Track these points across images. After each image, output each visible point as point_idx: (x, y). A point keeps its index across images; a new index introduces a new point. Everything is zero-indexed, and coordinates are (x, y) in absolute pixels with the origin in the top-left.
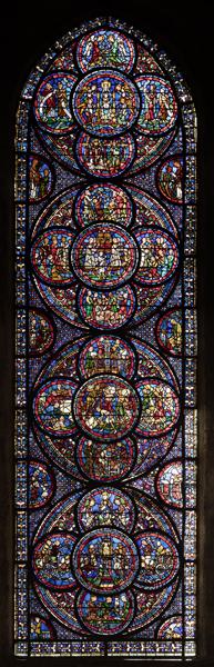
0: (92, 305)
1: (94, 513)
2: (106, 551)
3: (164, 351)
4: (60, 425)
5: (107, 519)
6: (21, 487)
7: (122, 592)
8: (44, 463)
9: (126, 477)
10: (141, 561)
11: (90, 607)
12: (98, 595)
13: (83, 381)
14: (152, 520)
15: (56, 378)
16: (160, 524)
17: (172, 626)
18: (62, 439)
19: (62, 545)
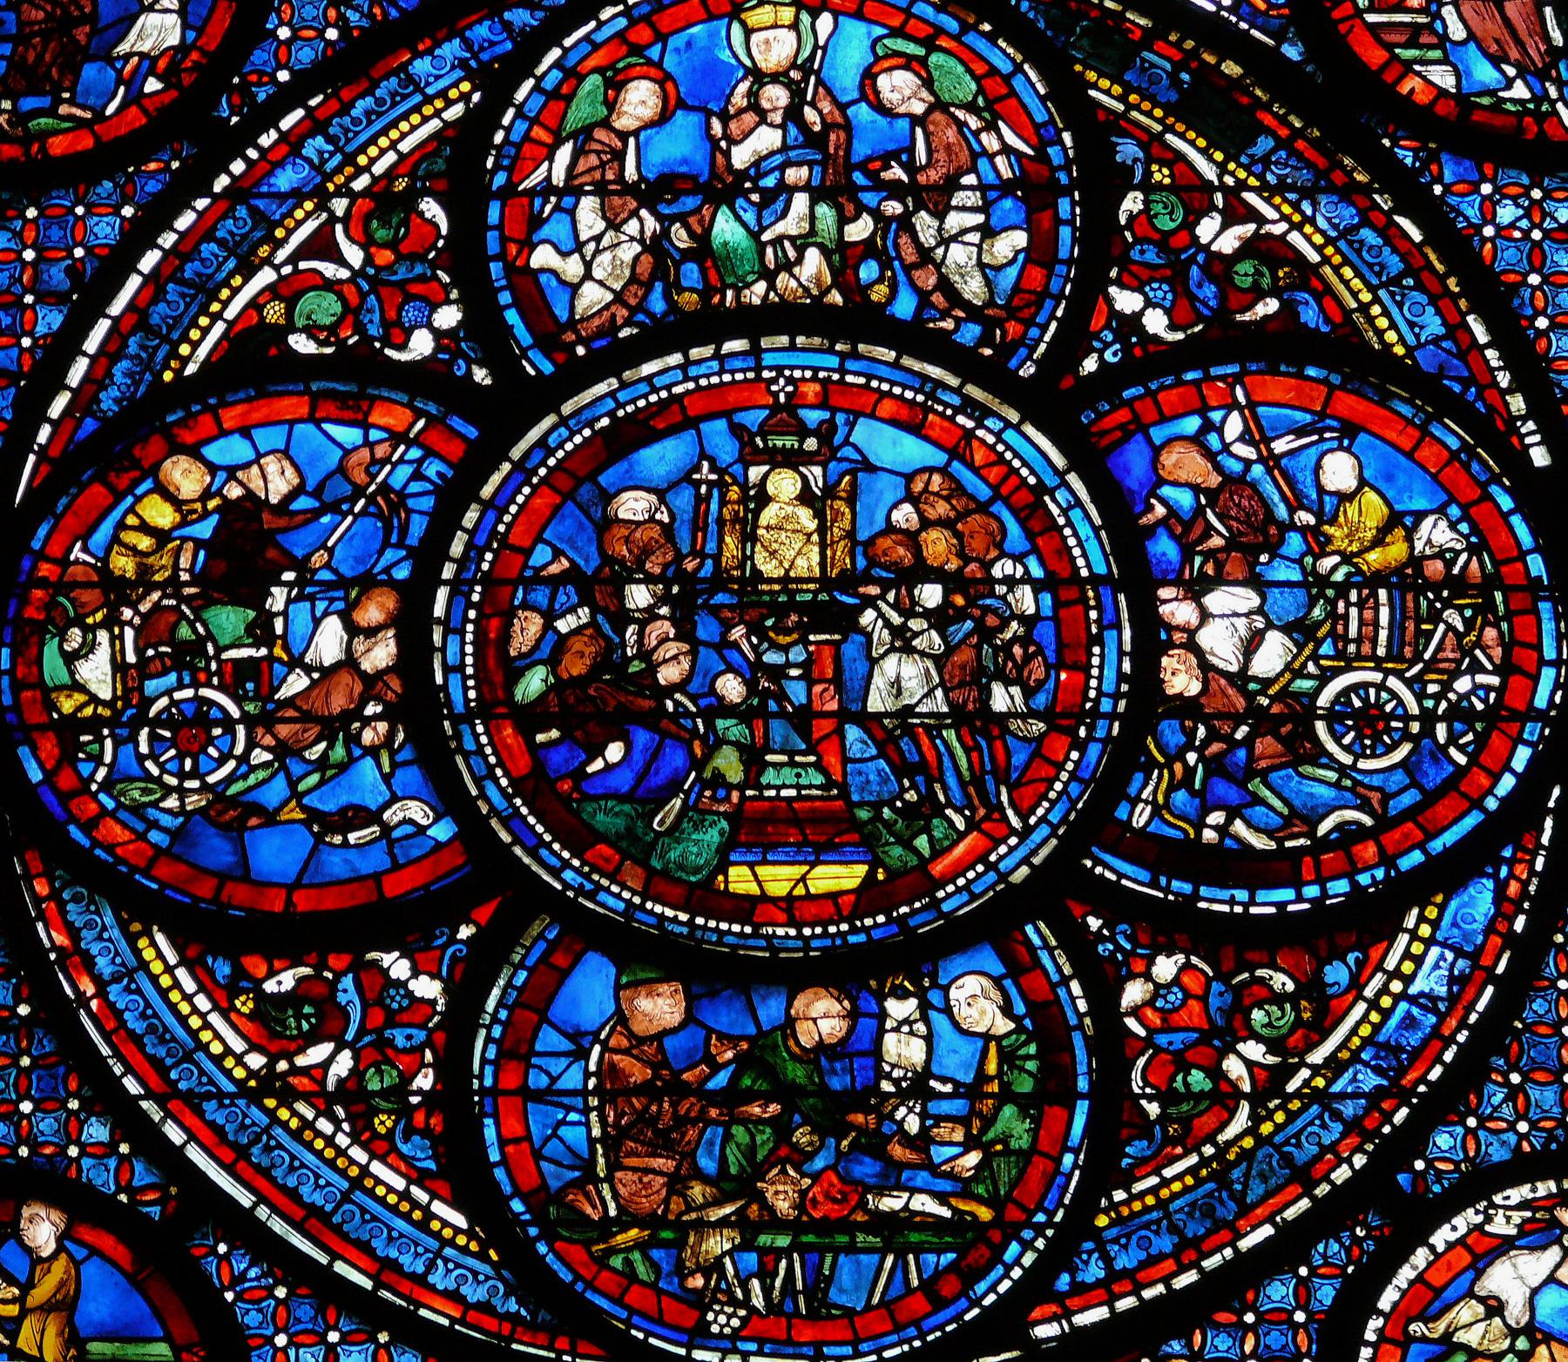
1: (657, 191)
2: (789, 545)
5: (796, 242)
7: (958, 936)
10: (1153, 638)
11: (611, 1087)
12: (703, 972)
14: (1262, 249)
16: (1351, 288)
17: (1508, 1280)
19: (329, 493)
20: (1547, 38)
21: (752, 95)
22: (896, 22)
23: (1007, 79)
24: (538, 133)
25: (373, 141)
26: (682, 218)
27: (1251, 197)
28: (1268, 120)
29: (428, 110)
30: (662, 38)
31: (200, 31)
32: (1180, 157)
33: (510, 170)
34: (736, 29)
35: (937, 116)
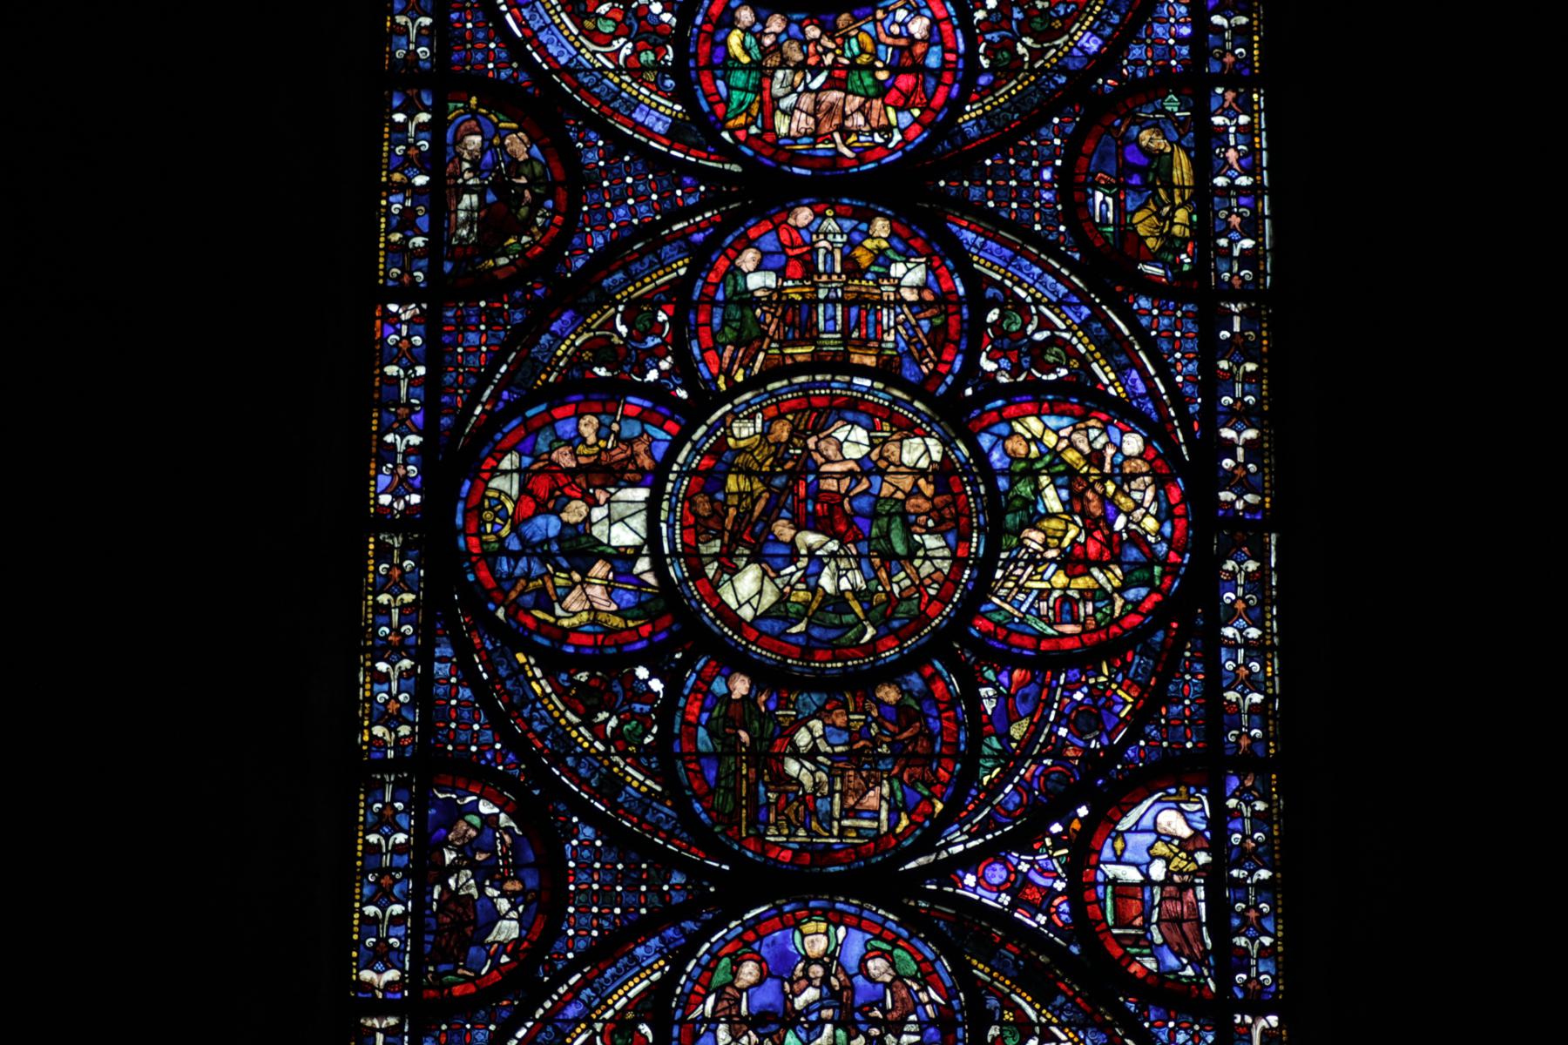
0: (755, 66)
3: (1107, 267)
4: (586, 601)
6: (383, 896)
8: (505, 781)
9: (926, 844)
13: (706, 399)
15: (578, 390)
18: (597, 665)
20: (1204, 944)
21: (805, 970)
22: (877, 931)
23: (932, 963)
24: (698, 988)
25: (615, 991)
26: (769, 1036)
27: (1055, 1030)
28: (1063, 986)
29: (643, 975)
30: (760, 938)
31: (529, 931)
32: (1019, 1006)
33: (684, 1008)
34: (797, 935)
35: (897, 983)
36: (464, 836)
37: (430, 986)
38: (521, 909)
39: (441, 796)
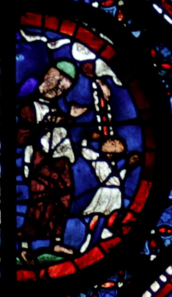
8: (101, 21)
31: (132, 200)
36: (56, 88)
37: (24, 266)
38: (123, 174)
39: (29, 39)
